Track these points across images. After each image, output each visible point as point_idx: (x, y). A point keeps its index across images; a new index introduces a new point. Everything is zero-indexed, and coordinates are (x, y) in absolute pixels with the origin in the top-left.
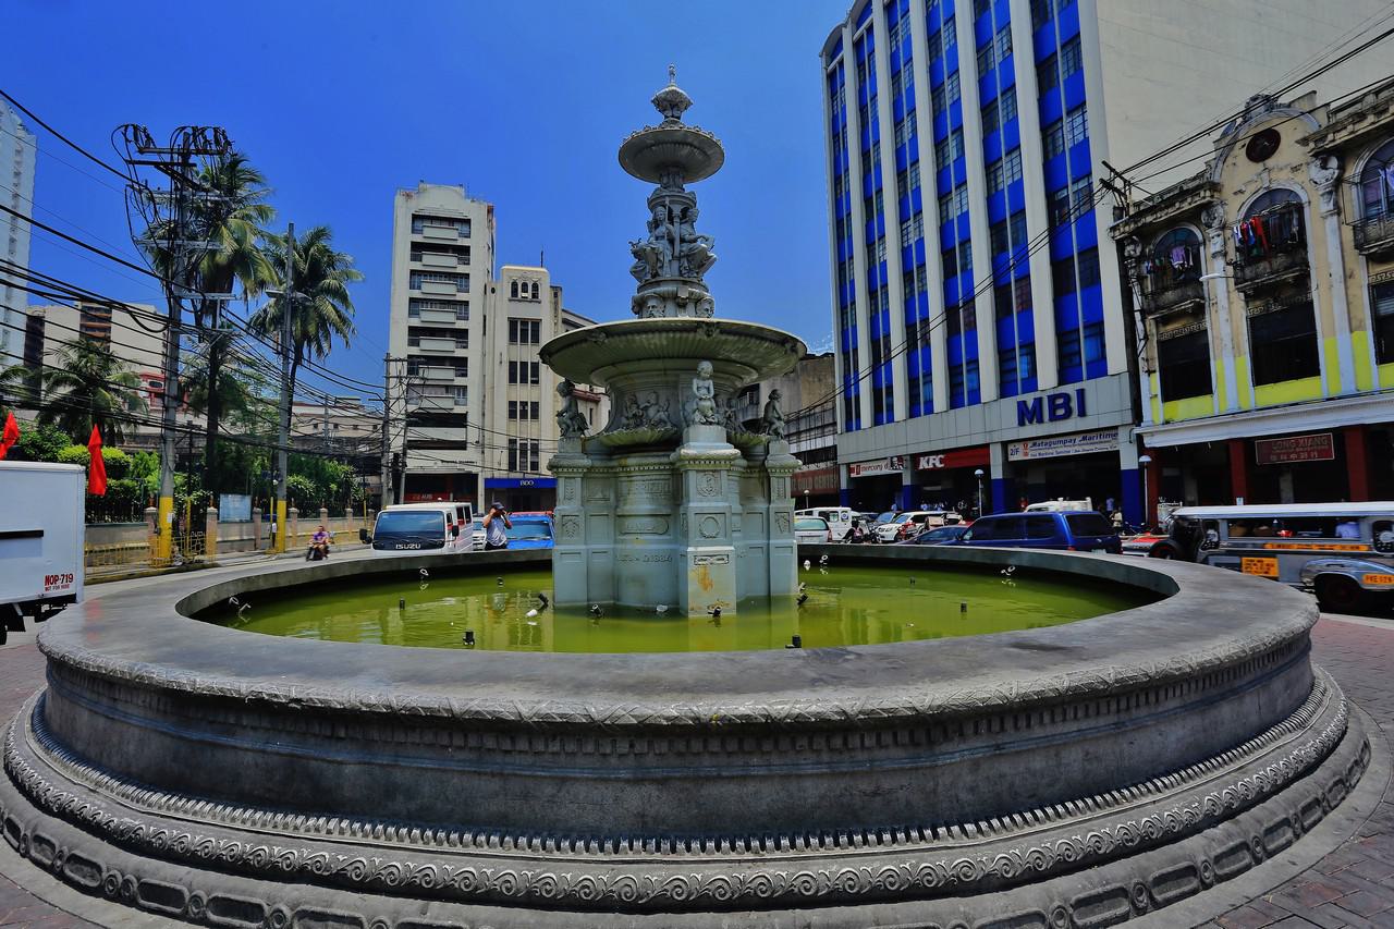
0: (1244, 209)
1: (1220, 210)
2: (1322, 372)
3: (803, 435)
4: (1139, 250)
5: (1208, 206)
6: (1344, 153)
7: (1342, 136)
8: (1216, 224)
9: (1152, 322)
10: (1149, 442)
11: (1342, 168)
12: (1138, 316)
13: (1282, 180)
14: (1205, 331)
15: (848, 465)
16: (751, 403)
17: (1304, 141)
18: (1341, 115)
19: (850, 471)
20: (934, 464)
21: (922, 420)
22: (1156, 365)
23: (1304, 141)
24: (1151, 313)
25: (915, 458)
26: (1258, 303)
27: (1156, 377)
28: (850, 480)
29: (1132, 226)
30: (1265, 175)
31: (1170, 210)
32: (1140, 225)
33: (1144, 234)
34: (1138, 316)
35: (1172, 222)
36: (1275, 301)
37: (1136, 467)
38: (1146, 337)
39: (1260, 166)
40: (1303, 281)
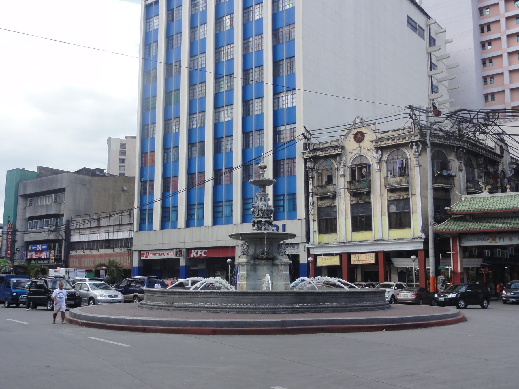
0: (352, 160)
1: (344, 158)
2: (373, 229)
3: (102, 229)
4: (313, 165)
5: (339, 155)
6: (382, 149)
7: (383, 144)
8: (342, 162)
9: (316, 199)
10: (312, 252)
11: (382, 155)
12: (310, 194)
13: (364, 152)
14: (336, 206)
15: (140, 251)
16: (55, 202)
17: (372, 142)
18: (383, 135)
19: (141, 255)
20: (201, 255)
21: (195, 230)
22: (316, 218)
23: (372, 142)
24: (316, 195)
25: (189, 250)
26: (354, 199)
27: (316, 224)
28: (140, 261)
29: (311, 155)
30: (359, 148)
31: (326, 152)
32: (314, 155)
33: (316, 159)
34: (310, 194)
35: (327, 157)
36: (360, 199)
37: (306, 262)
38: (313, 204)
39: (357, 145)
40: (369, 193)
